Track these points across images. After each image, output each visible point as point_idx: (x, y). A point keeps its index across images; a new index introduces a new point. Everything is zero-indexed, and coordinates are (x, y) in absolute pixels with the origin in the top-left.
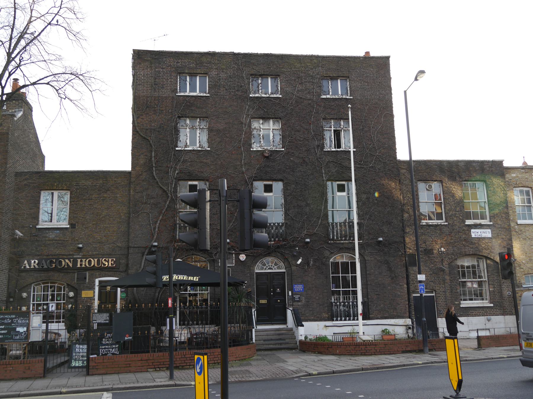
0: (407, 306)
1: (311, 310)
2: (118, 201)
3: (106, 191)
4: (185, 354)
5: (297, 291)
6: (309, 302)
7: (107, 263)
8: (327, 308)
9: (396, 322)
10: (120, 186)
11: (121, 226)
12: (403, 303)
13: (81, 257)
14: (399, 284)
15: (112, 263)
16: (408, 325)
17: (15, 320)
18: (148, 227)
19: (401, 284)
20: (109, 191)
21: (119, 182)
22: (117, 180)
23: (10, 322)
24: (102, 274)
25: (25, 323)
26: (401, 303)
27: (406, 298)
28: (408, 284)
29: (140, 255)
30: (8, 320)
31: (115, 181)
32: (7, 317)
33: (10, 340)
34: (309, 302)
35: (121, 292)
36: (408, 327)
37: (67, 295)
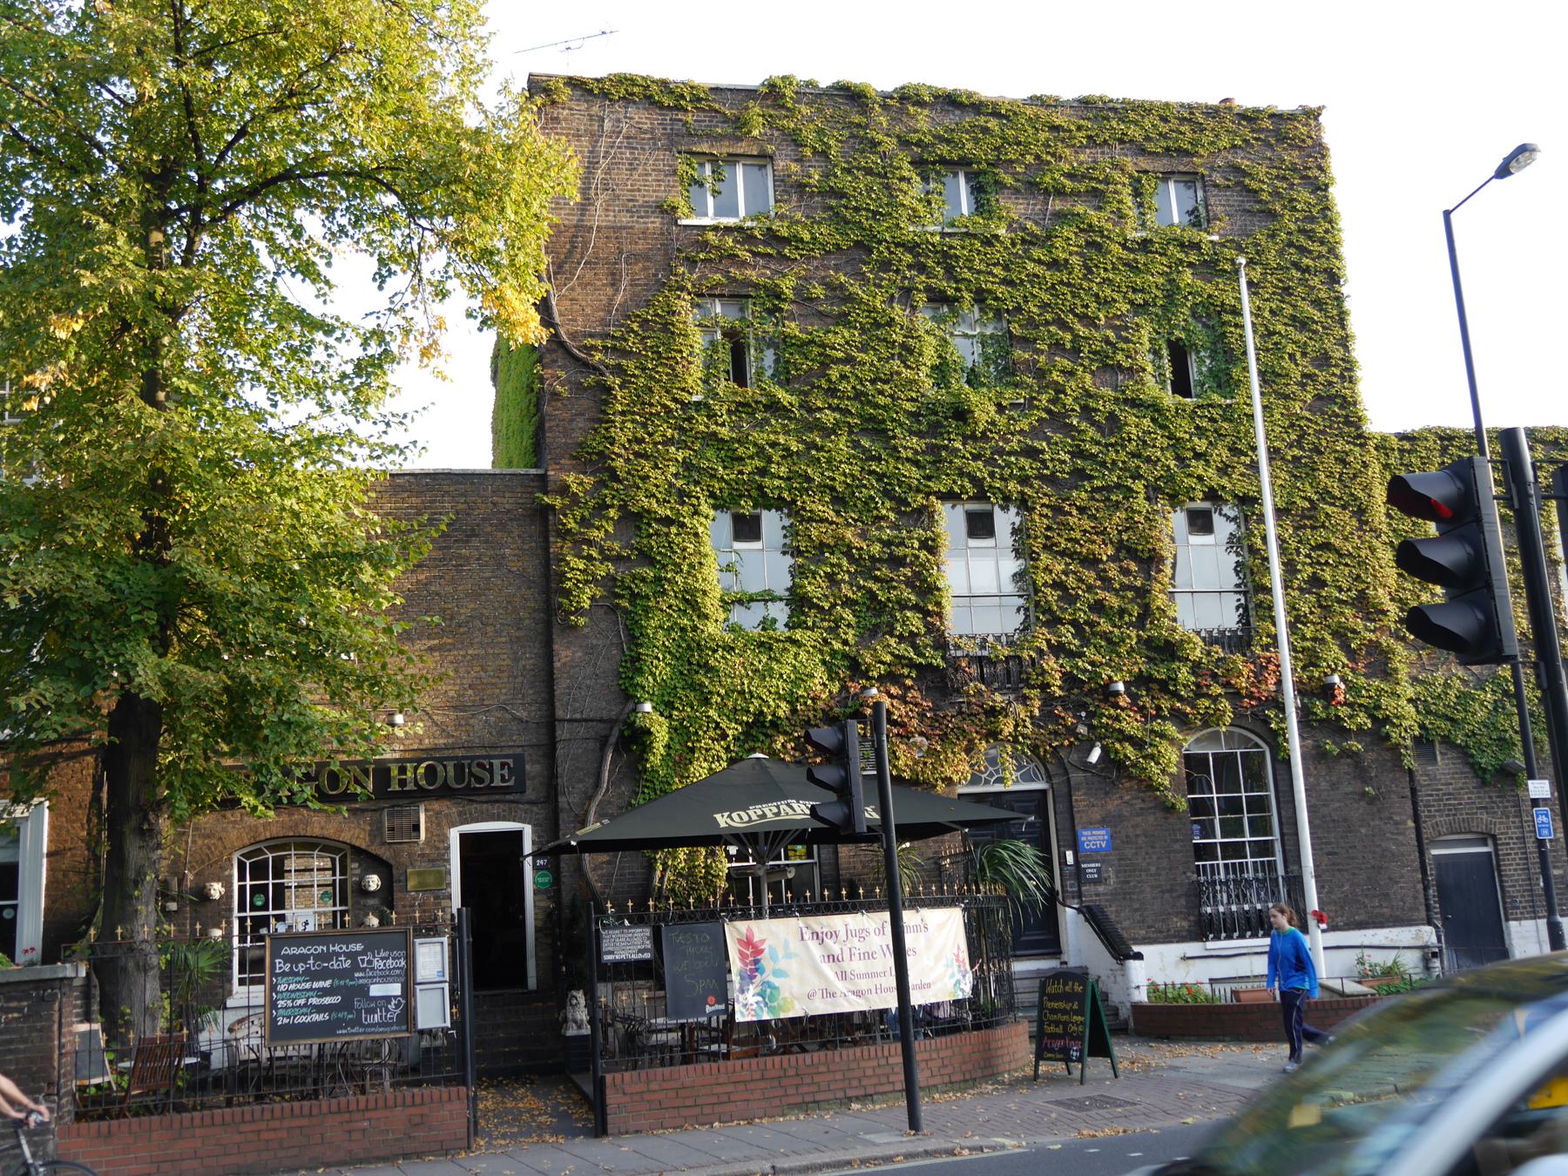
0: (1420, 886)
1: (1137, 910)
4: (886, 1053)
5: (1091, 850)
6: (1128, 882)
8: (1183, 902)
9: (1390, 936)
10: (511, 520)
12: (1407, 884)
13: (397, 756)
14: (1391, 818)
16: (1428, 947)
17: (363, 961)
18: (614, 652)
19: (1397, 818)
20: (477, 536)
22: (499, 500)
23: (347, 965)
26: (1402, 877)
27: (1413, 861)
28: (1416, 818)
29: (592, 745)
30: (343, 958)
31: (495, 504)
32: (337, 948)
34: (1128, 882)
35: (536, 868)
36: (1428, 955)
37: (359, 883)
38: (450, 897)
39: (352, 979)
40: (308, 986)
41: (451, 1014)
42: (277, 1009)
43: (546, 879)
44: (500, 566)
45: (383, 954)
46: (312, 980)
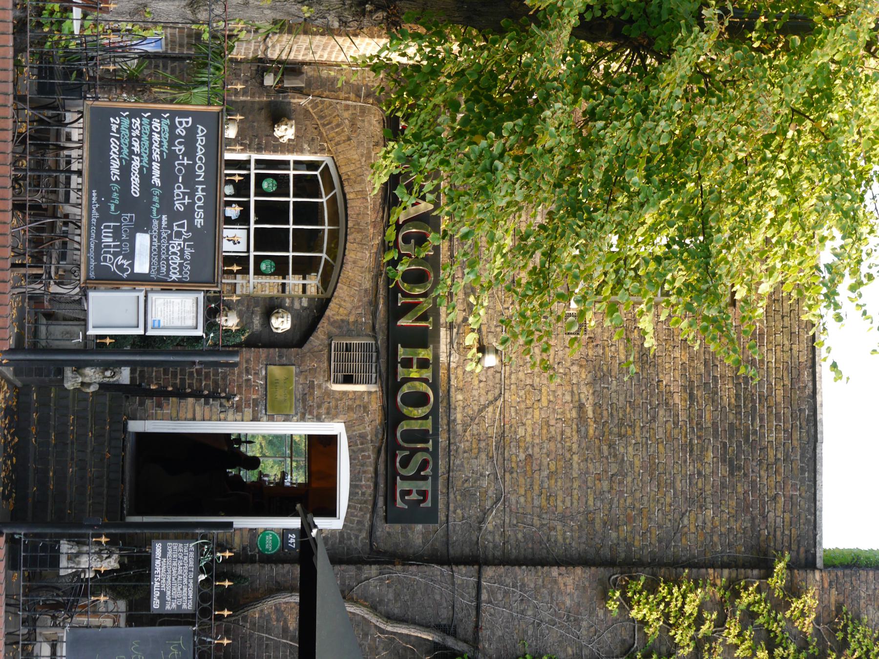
2: (683, 514)
3: (731, 460)
7: (410, 471)
10: (753, 519)
11: (572, 531)
13: (443, 358)
15: (409, 492)
17: (182, 226)
20: (731, 473)
21: (771, 514)
23: (178, 205)
24: (363, 450)
25: (168, 265)
29: (444, 614)
30: (186, 201)
31: (775, 498)
32: (200, 194)
33: (97, 210)
35: (285, 532)
38: (255, 419)
39: (159, 212)
40: (156, 156)
41: (104, 337)
42: (130, 117)
43: (270, 546)
44: (690, 501)
45: (188, 252)
46: (162, 162)
